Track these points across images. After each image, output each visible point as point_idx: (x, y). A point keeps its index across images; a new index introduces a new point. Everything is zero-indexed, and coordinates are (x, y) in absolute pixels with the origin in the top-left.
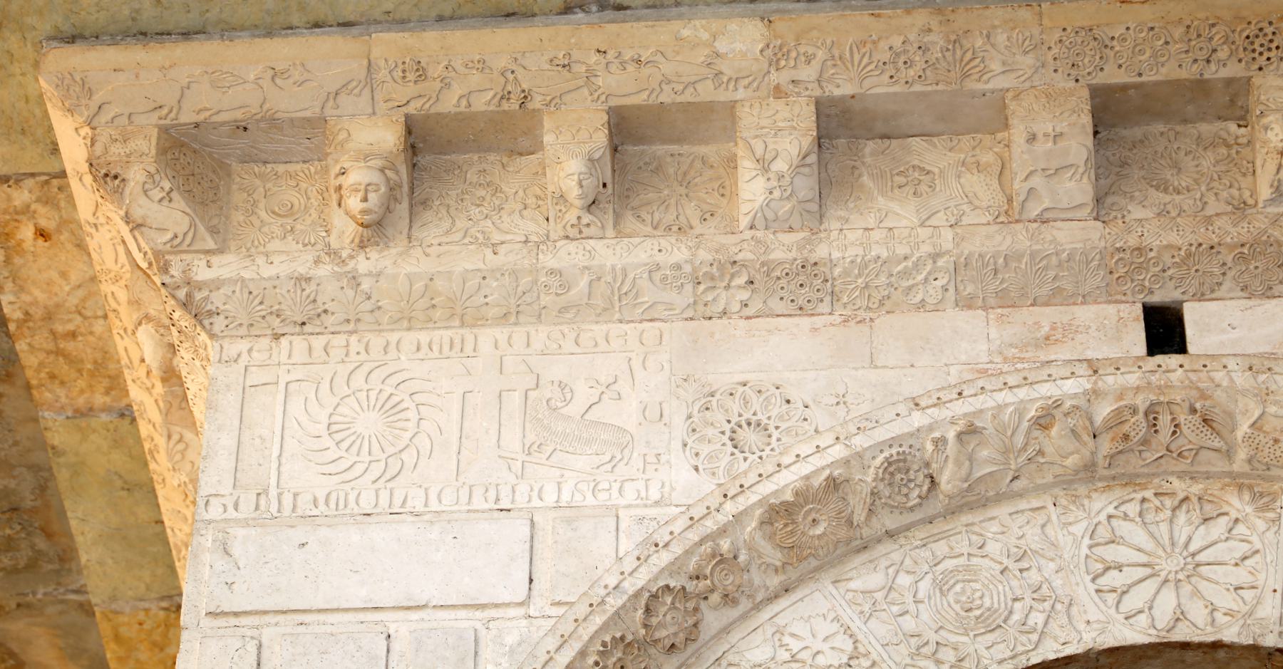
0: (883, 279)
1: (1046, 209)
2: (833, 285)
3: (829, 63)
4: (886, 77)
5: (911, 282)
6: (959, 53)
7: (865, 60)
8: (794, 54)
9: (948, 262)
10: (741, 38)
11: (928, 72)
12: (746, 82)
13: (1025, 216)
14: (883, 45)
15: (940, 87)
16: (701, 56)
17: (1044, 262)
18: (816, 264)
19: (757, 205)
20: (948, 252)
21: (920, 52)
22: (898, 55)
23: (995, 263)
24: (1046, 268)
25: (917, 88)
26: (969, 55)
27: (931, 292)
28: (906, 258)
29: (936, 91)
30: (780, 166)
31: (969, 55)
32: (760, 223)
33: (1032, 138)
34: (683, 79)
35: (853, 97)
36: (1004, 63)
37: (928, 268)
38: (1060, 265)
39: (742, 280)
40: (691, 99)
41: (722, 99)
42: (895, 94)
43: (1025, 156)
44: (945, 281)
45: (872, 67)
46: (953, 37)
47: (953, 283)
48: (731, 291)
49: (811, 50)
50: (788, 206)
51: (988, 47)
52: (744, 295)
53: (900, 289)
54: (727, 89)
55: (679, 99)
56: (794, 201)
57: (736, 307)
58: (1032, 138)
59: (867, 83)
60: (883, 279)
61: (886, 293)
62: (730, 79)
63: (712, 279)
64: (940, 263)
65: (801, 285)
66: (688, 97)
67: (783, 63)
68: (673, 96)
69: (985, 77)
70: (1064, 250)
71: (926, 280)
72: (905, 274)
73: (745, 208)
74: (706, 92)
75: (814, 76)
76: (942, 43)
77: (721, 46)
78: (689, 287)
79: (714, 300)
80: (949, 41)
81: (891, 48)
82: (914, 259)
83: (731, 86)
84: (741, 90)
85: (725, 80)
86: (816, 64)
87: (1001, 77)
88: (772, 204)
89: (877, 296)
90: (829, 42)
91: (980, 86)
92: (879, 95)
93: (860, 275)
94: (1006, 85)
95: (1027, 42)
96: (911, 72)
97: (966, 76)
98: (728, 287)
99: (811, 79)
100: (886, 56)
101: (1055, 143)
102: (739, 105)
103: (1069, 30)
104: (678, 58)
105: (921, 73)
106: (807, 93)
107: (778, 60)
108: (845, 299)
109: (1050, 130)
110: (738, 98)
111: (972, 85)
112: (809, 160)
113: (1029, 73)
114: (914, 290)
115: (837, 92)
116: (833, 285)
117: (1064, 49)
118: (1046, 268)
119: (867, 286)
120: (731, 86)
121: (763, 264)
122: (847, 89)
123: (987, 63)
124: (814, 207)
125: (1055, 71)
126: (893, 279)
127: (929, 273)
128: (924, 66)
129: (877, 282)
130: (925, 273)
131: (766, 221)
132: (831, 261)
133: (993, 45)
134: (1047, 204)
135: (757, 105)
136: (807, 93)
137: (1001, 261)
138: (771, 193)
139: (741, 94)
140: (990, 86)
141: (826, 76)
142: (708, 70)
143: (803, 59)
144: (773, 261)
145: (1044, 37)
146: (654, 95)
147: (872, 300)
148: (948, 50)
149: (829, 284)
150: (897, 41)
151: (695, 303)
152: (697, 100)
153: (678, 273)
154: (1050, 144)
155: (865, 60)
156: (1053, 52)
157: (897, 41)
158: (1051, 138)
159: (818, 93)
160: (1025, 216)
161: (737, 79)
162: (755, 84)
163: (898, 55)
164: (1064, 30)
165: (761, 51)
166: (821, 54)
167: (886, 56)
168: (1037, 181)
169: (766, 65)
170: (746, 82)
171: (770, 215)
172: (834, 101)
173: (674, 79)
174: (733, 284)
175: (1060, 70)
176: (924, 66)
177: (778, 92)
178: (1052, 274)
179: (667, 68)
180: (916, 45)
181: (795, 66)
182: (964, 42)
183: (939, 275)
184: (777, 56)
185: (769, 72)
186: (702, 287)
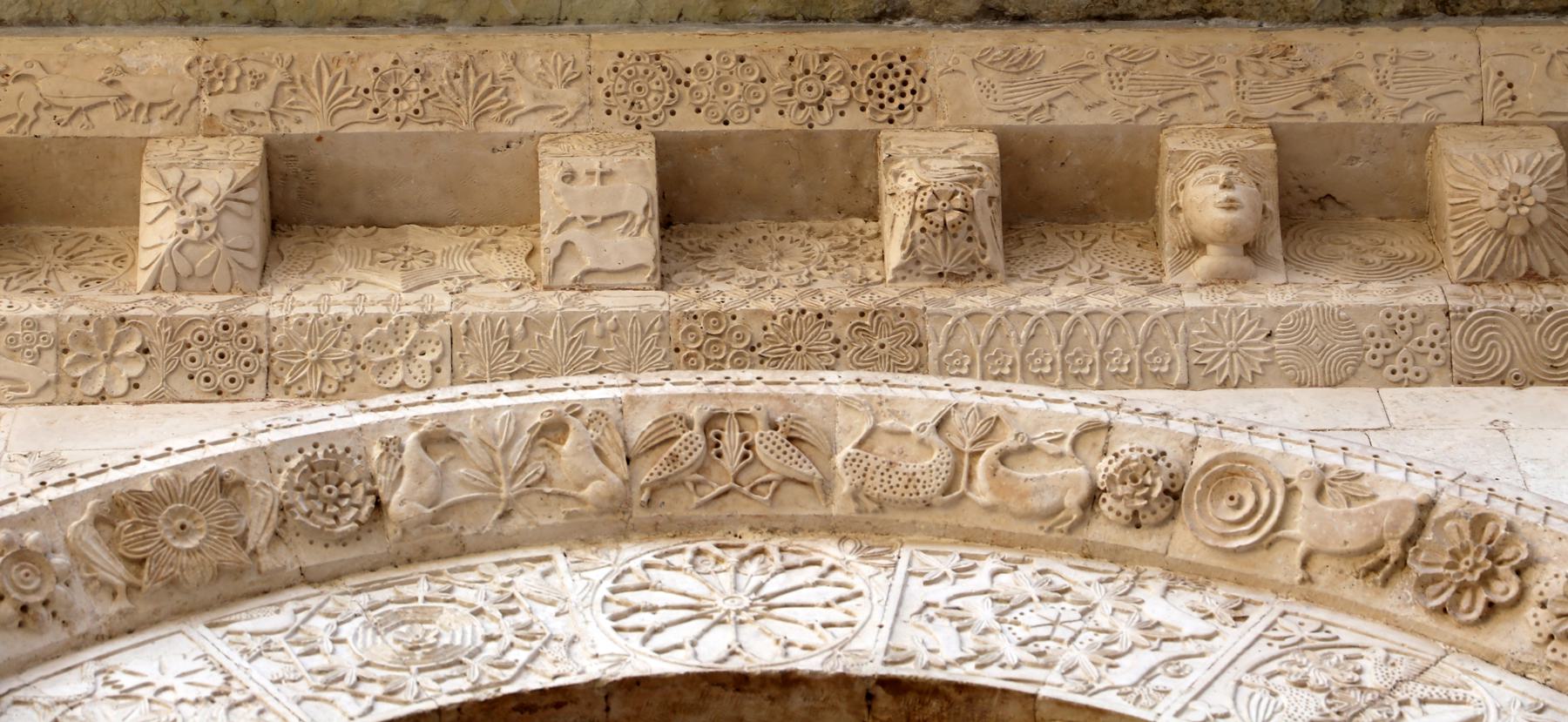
0: (345, 350)
1: (588, 272)
2: (270, 359)
3: (287, 89)
4: (368, 113)
5: (386, 357)
6: (472, 80)
7: (339, 85)
8: (236, 73)
9: (441, 327)
10: (160, 57)
11: (428, 106)
12: (165, 110)
13: (557, 282)
14: (366, 65)
15: (445, 128)
16: (98, 70)
17: (582, 331)
18: (245, 325)
19: (163, 249)
20: (442, 315)
21: (418, 77)
22: (386, 80)
23: (510, 331)
24: (584, 339)
25: (412, 128)
26: (487, 85)
27: (416, 371)
28: (379, 321)
29: (439, 133)
30: (202, 197)
31: (487, 85)
32: (167, 280)
33: (569, 177)
34: (68, 102)
35: (319, 139)
36: (535, 97)
37: (412, 335)
38: (603, 336)
39: (131, 347)
40: (79, 132)
41: (128, 134)
42: (381, 136)
43: (560, 200)
44: (435, 356)
45: (348, 95)
46: (464, 58)
47: (448, 359)
48: (115, 364)
49: (260, 69)
50: (210, 252)
51: (514, 74)
52: (135, 369)
53: (369, 368)
54: (135, 120)
55: (62, 132)
56: (218, 245)
57: (120, 387)
58: (569, 177)
59: (342, 118)
60: (345, 350)
61: (349, 371)
62: (140, 106)
63: (87, 344)
64: (431, 328)
65: (222, 356)
66: (75, 129)
67: (220, 85)
68: (54, 127)
69: (510, 116)
70: (611, 314)
71: (409, 355)
72: (377, 344)
73: (145, 258)
74: (105, 123)
75: (264, 105)
76: (448, 65)
77: (131, 59)
78: (50, 357)
79: (88, 376)
80: (459, 65)
81: (376, 70)
82: (392, 321)
83: (142, 116)
84: (157, 122)
85: (133, 106)
86: (267, 90)
87: (533, 117)
88: (188, 249)
89: (336, 374)
90: (287, 58)
91: (502, 128)
92: (356, 136)
93: (311, 344)
94: (539, 129)
95: (569, 69)
96: (404, 105)
97: (481, 114)
98: (109, 359)
99: (260, 109)
100: (369, 81)
101: (602, 183)
102: (150, 145)
103: (627, 56)
104: (66, 72)
105: (418, 106)
106: (252, 130)
107: (212, 82)
108: (287, 380)
109: (596, 166)
110: (152, 133)
111: (489, 126)
112: (244, 195)
113: (571, 112)
114: (391, 368)
115: (297, 130)
116: (270, 359)
117: (620, 81)
118: (584, 339)
119: (320, 361)
120: (142, 116)
121: (165, 322)
122: (313, 127)
123: (512, 96)
124: (253, 261)
125: (609, 113)
126: (360, 352)
127: (414, 345)
128: (423, 96)
129: (336, 355)
130: (407, 343)
131: (176, 277)
132: (268, 321)
133: (521, 72)
134: (589, 263)
135: (179, 141)
136: (252, 130)
137: (518, 327)
138: (185, 232)
139: (156, 127)
140: (516, 128)
141: (282, 106)
142: (108, 90)
143: (249, 80)
144: (181, 318)
145: (592, 63)
146: (25, 126)
147: (328, 382)
148: (457, 76)
149: (263, 356)
150: (385, 62)
151: (58, 380)
152: (91, 133)
153: (35, 333)
154: (596, 184)
155: (339, 85)
156: (604, 85)
157: (385, 62)
158: (597, 176)
159: (268, 129)
160: (557, 282)
161: (151, 106)
162: (178, 115)
163: (386, 80)
164: (621, 55)
165: (189, 67)
166: (275, 76)
167: (369, 81)
168: (575, 233)
169: (196, 86)
170: (165, 110)
171: (184, 269)
172: (288, 141)
173: (58, 102)
174: (119, 353)
175: (614, 111)
176: (423, 96)
177: (211, 128)
178: (593, 348)
179: (48, 86)
180: (412, 67)
181: (236, 91)
182: (481, 66)
183: (428, 347)
184: (211, 77)
185: (198, 97)
186: (69, 358)
